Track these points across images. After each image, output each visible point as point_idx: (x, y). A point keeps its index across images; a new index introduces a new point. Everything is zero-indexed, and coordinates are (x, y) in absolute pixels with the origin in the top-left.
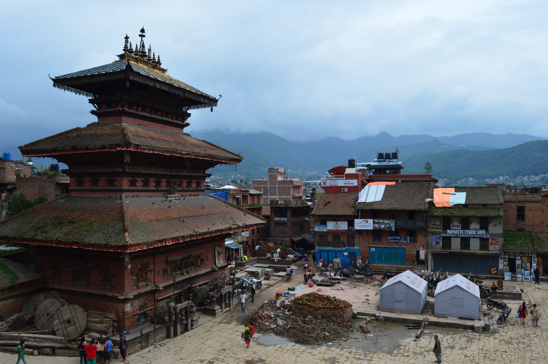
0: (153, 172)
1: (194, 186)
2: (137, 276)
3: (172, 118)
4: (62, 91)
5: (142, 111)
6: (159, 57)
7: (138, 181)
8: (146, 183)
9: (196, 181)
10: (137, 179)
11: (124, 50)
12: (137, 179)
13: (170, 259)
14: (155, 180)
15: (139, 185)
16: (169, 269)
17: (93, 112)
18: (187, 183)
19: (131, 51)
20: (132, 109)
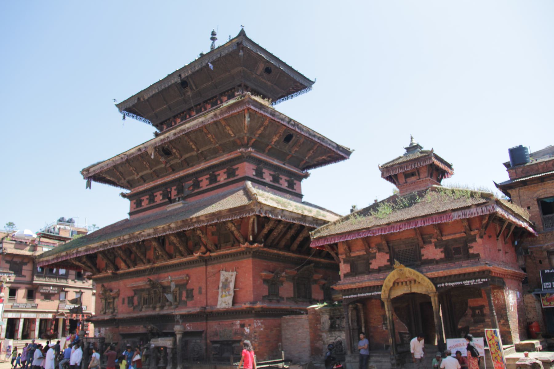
0: (159, 182)
1: (222, 179)
7: (143, 200)
8: (152, 199)
12: (142, 198)
14: (161, 192)
15: (145, 204)
16: (136, 298)
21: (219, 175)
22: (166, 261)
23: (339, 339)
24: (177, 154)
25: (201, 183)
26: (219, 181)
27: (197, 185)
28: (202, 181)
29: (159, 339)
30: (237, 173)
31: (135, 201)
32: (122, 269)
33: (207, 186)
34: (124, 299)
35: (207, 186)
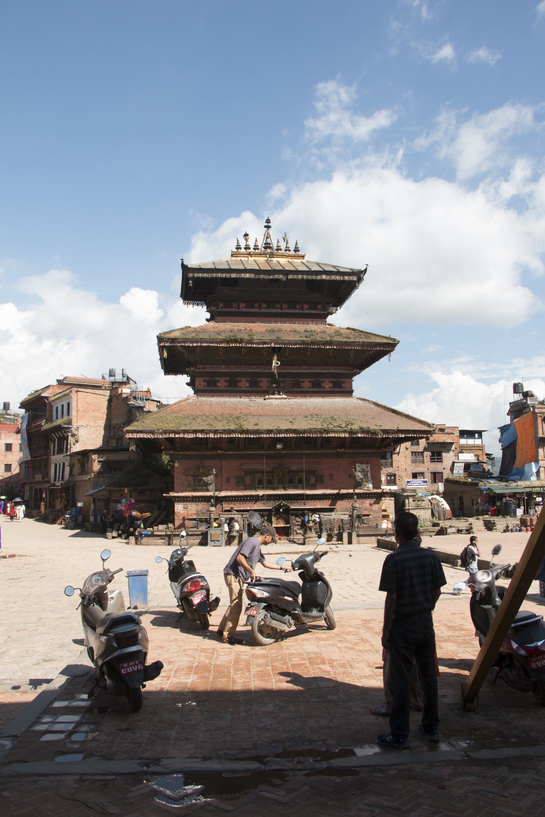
1: (327, 386)
2: (194, 478)
3: (302, 308)
4: (195, 307)
5: (246, 307)
6: (296, 243)
7: (219, 381)
9: (332, 380)
10: (218, 379)
11: (237, 248)
13: (244, 467)
16: (248, 479)
17: (208, 320)
18: (313, 382)
19: (247, 248)
20: (232, 307)
21: (324, 382)
22: (293, 450)
23: (419, 513)
24: (287, 354)
25: (302, 384)
26: (324, 387)
27: (298, 384)
28: (303, 382)
29: (333, 513)
30: (343, 385)
31: (207, 379)
32: (228, 450)
33: (309, 387)
34: (228, 479)
35: (309, 387)
